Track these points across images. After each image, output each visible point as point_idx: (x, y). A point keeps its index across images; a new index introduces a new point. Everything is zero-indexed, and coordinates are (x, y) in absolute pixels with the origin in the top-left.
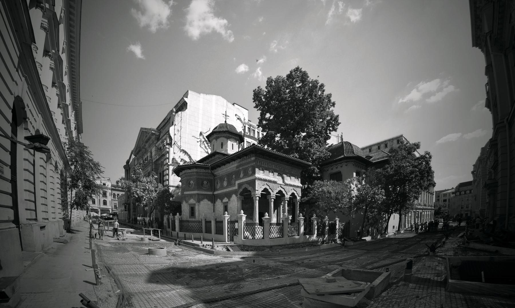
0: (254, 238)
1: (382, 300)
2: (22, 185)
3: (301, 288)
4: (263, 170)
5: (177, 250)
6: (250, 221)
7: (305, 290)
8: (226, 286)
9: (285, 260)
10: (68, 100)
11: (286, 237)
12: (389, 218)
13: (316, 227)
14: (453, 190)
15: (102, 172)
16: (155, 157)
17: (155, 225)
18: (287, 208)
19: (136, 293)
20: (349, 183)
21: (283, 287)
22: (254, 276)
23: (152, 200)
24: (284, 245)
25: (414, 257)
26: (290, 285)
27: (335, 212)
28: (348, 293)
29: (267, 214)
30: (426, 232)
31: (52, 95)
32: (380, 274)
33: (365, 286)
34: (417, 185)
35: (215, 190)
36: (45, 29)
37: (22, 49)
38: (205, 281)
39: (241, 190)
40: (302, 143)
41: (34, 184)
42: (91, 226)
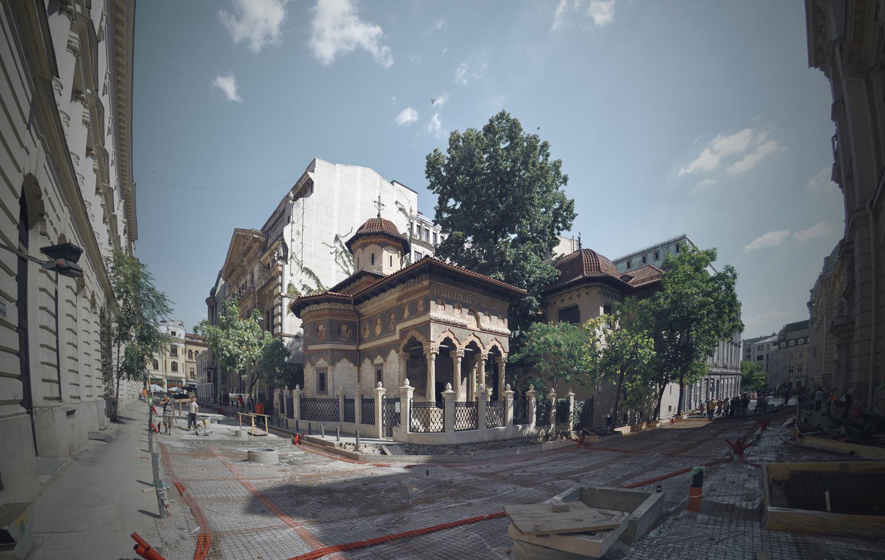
0: (427, 431)
1: (649, 546)
2: (37, 337)
3: (509, 523)
4: (443, 304)
5: (296, 453)
6: (420, 400)
7: (515, 526)
8: (380, 519)
9: (480, 471)
10: (113, 182)
11: (482, 427)
12: (662, 391)
13: (535, 410)
14: (775, 338)
15: (169, 311)
16: (259, 283)
17: (258, 408)
18: (484, 374)
19: (227, 532)
20: (592, 326)
21: (478, 521)
22: (427, 501)
23: (254, 361)
24: (480, 443)
25: (706, 465)
26: (491, 517)
27: (567, 381)
28: (589, 533)
29: (449, 385)
30: (728, 417)
31: (85, 170)
32: (645, 496)
33: (619, 518)
34: (710, 329)
35: (361, 341)
36: (74, 51)
37: (37, 89)
38: (345, 509)
39: (405, 341)
41: (56, 333)
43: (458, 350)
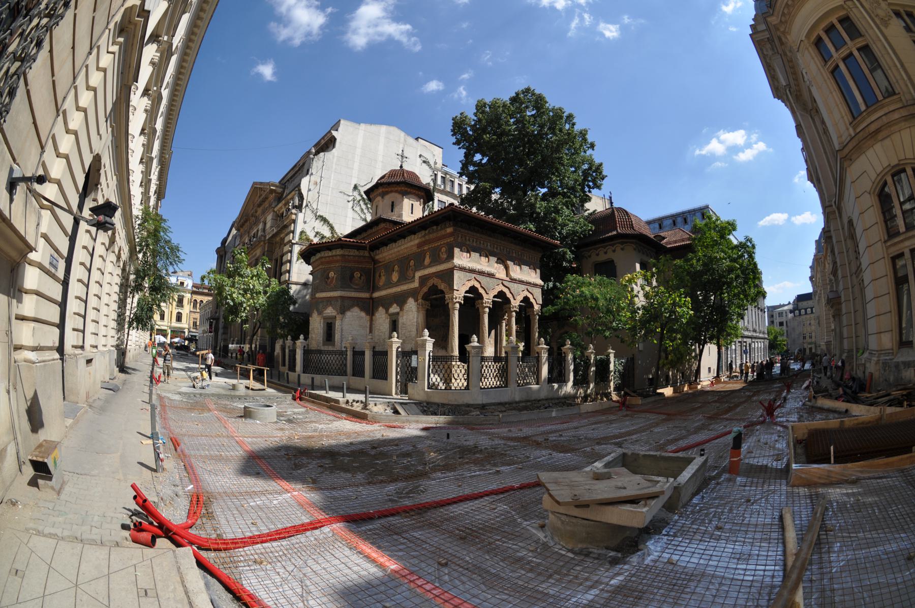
4: (468, 252)
6: (441, 353)
8: (391, 488)
9: (510, 435)
11: (512, 386)
13: (572, 367)
17: (260, 357)
18: (514, 327)
22: (447, 468)
23: (257, 310)
24: (510, 403)
27: (606, 338)
29: (475, 338)
38: (349, 475)
39: (425, 289)
40: (541, 207)
42: (155, 360)
43: (485, 300)
